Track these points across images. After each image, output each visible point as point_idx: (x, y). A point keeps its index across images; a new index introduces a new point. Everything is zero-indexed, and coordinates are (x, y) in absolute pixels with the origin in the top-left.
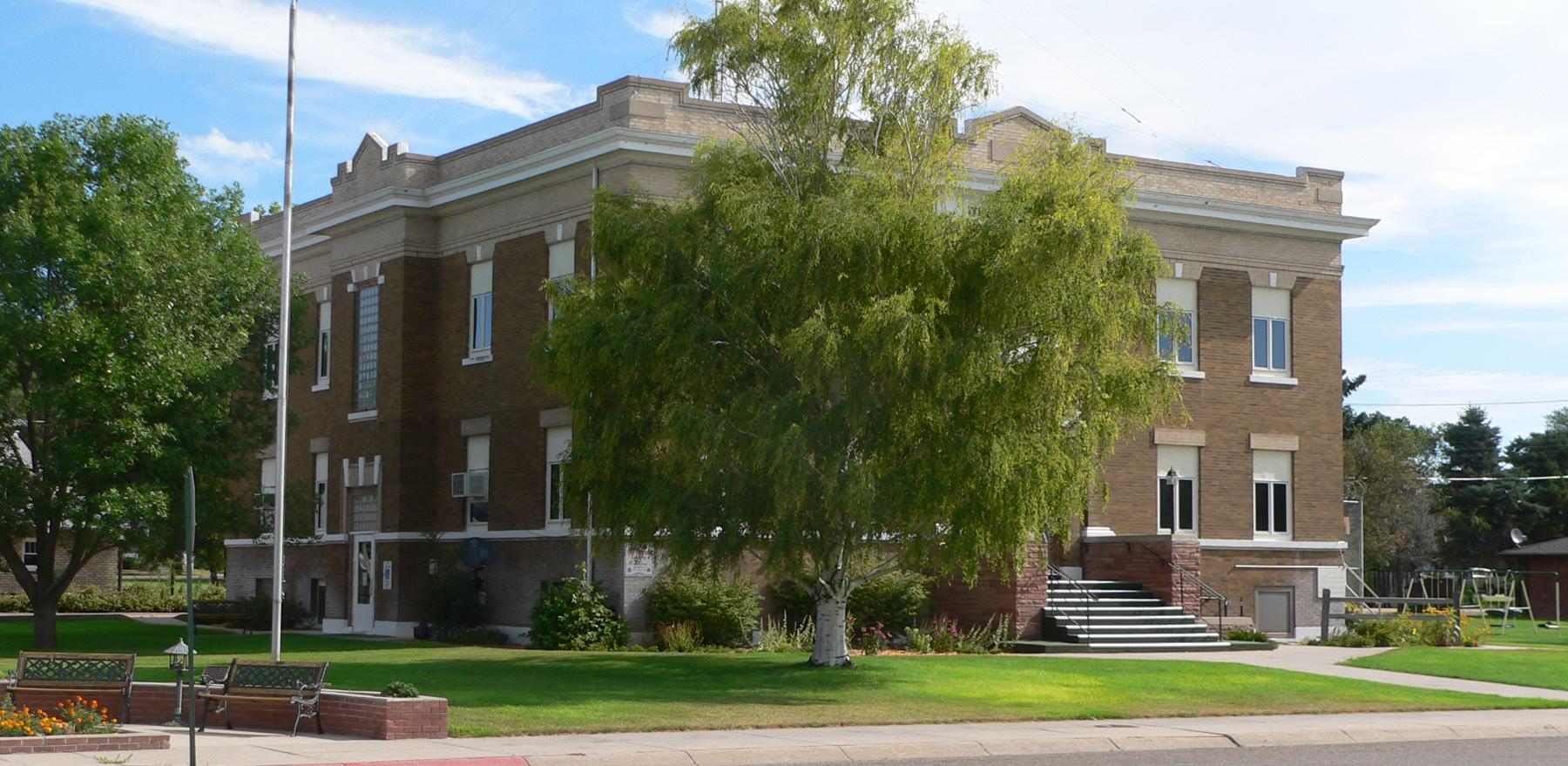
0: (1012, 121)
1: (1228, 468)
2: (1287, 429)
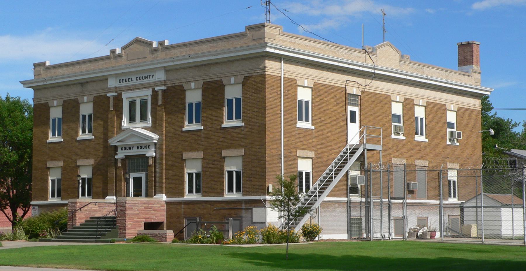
0: (135, 44)
1: (213, 166)
2: (240, 146)
